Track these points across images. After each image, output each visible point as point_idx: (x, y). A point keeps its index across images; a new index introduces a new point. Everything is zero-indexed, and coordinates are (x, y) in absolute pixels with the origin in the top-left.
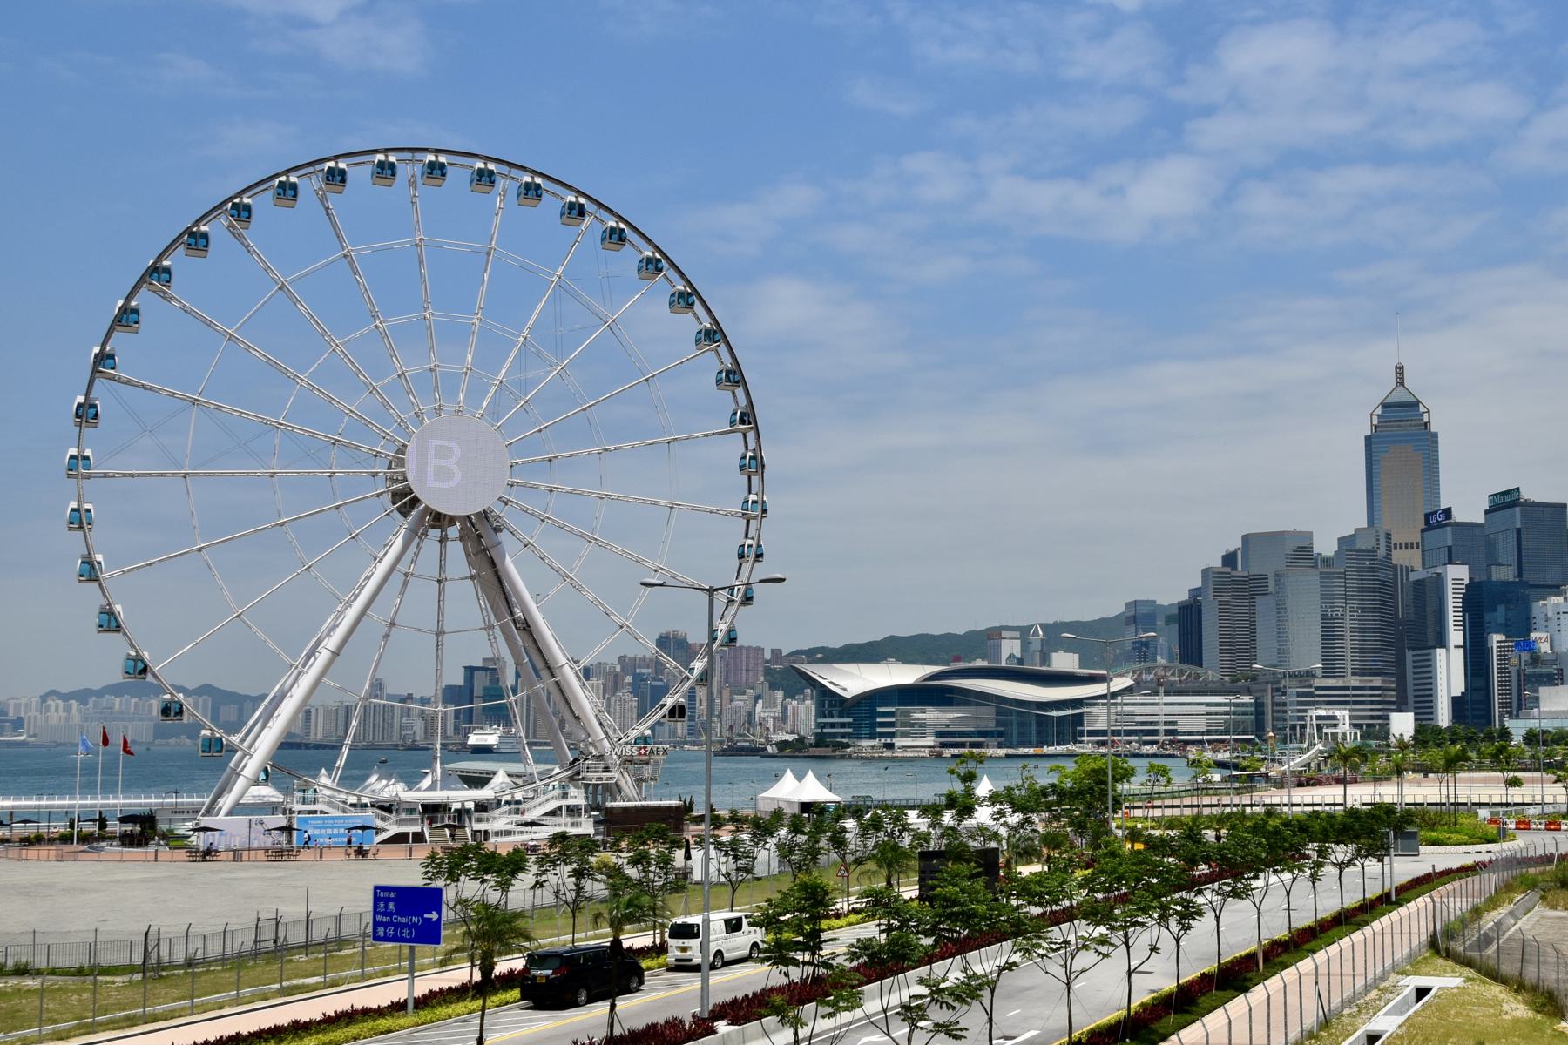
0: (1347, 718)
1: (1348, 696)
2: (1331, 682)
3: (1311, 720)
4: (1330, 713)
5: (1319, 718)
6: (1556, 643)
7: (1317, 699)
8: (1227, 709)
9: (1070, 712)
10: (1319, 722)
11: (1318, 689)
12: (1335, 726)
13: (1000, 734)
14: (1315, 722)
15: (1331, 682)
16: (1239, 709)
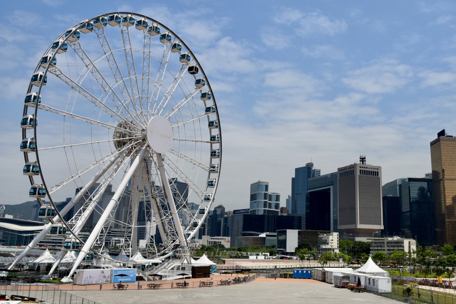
0: (124, 241)
1: (121, 234)
2: (116, 230)
3: (113, 240)
4: (119, 239)
5: (115, 240)
6: (184, 222)
7: (112, 234)
8: (83, 236)
9: (30, 235)
10: (116, 242)
11: (112, 231)
12: (120, 243)
13: (3, 241)
14: (114, 242)
15: (116, 230)
16: (85, 236)
